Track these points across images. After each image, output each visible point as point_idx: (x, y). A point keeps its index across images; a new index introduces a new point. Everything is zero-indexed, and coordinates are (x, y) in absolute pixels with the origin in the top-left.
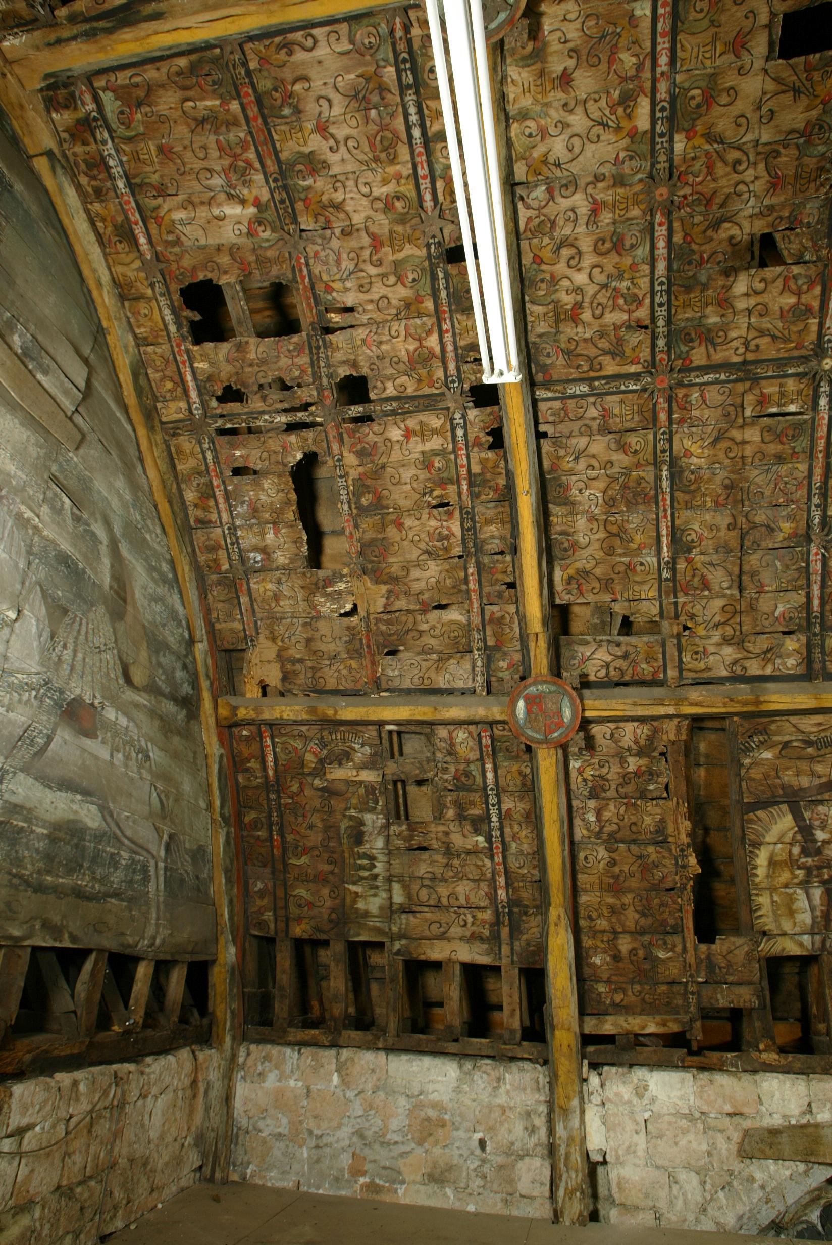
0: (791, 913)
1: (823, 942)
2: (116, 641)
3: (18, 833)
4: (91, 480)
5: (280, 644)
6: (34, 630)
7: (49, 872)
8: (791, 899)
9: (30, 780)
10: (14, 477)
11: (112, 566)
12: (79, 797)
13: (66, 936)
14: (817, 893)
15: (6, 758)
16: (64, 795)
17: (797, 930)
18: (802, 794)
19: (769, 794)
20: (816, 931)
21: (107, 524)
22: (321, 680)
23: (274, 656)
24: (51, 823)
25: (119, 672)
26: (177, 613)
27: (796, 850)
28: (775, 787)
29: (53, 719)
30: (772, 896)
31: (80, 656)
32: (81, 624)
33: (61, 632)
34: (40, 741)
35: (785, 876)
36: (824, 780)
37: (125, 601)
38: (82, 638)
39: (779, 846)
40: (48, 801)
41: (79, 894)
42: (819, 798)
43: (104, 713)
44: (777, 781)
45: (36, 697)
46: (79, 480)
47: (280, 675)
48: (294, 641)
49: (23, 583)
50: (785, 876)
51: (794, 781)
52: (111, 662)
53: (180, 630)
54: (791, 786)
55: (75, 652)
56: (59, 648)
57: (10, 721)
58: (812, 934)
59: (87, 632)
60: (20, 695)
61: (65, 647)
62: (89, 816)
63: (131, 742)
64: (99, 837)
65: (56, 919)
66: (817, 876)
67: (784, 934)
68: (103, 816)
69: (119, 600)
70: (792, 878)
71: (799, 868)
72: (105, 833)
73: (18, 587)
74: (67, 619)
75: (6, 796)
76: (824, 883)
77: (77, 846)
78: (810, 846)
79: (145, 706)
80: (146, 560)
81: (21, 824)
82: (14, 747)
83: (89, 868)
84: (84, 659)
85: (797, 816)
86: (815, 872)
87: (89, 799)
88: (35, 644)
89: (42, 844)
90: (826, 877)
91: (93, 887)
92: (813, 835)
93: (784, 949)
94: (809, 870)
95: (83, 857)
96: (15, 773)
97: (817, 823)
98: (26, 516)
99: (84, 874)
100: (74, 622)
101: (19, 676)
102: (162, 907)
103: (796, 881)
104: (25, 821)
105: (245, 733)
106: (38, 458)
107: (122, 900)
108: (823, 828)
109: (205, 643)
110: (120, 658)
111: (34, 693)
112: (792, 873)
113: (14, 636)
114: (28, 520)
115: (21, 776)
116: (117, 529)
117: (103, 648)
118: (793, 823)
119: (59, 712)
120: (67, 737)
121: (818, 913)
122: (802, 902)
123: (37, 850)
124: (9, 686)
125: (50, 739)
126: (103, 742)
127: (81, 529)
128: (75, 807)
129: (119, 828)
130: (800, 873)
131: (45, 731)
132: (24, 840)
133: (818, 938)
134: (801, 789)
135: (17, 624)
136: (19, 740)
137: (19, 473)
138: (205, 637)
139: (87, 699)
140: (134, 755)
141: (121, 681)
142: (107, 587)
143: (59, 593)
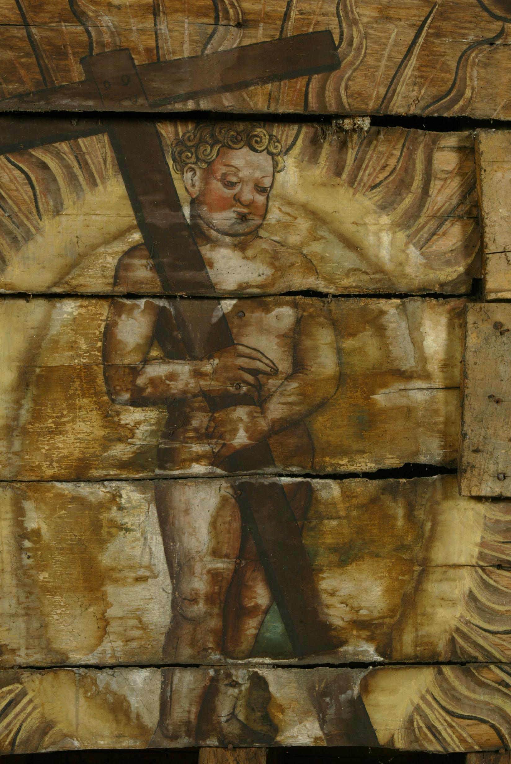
0: (94, 581)
1: (207, 699)
8: (97, 527)
14: (202, 504)
17: (112, 648)
18: (159, 83)
19: (29, 80)
20: (186, 653)
27: (133, 328)
28: (60, 53)
30: (19, 513)
35: (81, 430)
36: (260, 35)
39: (69, 308)
42: (228, 102)
44: (71, 29)
50: (81, 430)
51: (139, 34)
54: (124, 52)
58: (166, 666)
66: (204, 436)
67: (58, 666)
70: (107, 442)
71: (139, 401)
76: (231, 463)
78: (188, 312)
85: (146, 184)
86: (199, 420)
90: (241, 438)
92: (201, 264)
93: (46, 726)
94: (176, 410)
97: (223, 218)
103: (120, 451)
108: (244, 239)
112: (108, 418)
118: (126, 215)
121: (199, 584)
122: (139, 539)
130: (141, 421)
133: (187, 682)
134: (158, 64)
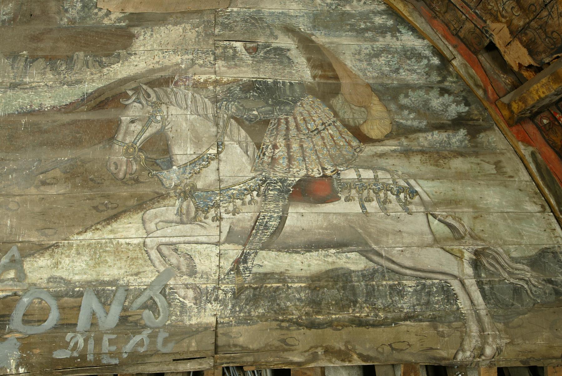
2: (336, 115)
3: (275, 292)
4: (259, 11)
5: (504, 20)
6: (239, 150)
7: (318, 313)
9: (273, 254)
10: (182, 63)
11: (309, 60)
12: (333, 251)
13: (355, 357)
15: (245, 245)
16: (315, 254)
21: (290, 30)
22: (555, 35)
23: (509, 36)
24: (307, 278)
25: (349, 136)
26: (413, 49)
29: (281, 203)
31: (295, 146)
32: (287, 122)
33: (267, 140)
34: (274, 223)
37: (336, 78)
38: (293, 132)
40: (299, 262)
41: (360, 323)
43: (342, 177)
45: (258, 195)
46: (245, 21)
47: (525, 51)
48: (509, 10)
49: (217, 125)
52: (337, 135)
53: (425, 62)
55: (288, 147)
56: (268, 153)
57: (239, 220)
59: (297, 127)
60: (242, 199)
61: (275, 147)
62: (353, 262)
63: (386, 188)
64: (369, 276)
65: (340, 346)
68: (367, 258)
69: (329, 82)
72: (375, 271)
73: (214, 129)
74: (270, 127)
75: (254, 270)
77: (344, 288)
79: (394, 151)
80: (350, 30)
81: (275, 285)
82: (250, 236)
83: (366, 301)
84: (301, 146)
87: (345, 249)
88: (245, 159)
89: (302, 294)
91: (376, 315)
95: (355, 294)
96: (256, 253)
98: (202, 81)
99: (361, 308)
100: (279, 123)
101: (237, 187)
102: (486, 319)
104: (279, 282)
105: (545, 121)
106: (198, 36)
107: (421, 321)
109: (459, 58)
110: (346, 125)
111: (255, 193)
113: (222, 164)
114: (206, 81)
115: (264, 253)
116: (303, 26)
117: (320, 128)
119: (286, 196)
120: (302, 211)
123: (300, 300)
124: (230, 197)
125: (283, 219)
126: (348, 199)
127: (262, 54)
128: (330, 260)
129: (393, 262)
131: (276, 215)
132: (284, 295)
135: (222, 155)
136: (253, 229)
137: (186, 57)
138: (455, 53)
139: (316, 174)
140: (392, 197)
141: (355, 143)
142: (310, 79)
143: (255, 113)
